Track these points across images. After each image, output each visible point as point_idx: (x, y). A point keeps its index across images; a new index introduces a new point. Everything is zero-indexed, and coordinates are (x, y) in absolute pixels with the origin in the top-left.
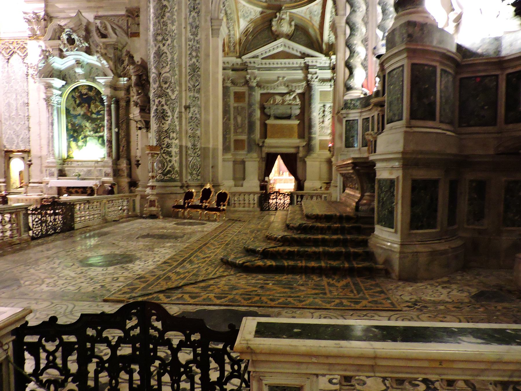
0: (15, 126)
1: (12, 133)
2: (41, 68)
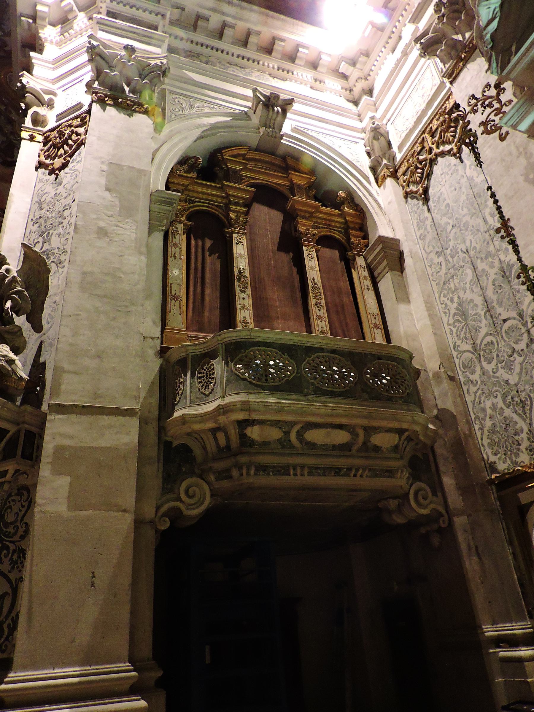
0: (503, 374)
1: (501, 404)
2: (494, 25)
